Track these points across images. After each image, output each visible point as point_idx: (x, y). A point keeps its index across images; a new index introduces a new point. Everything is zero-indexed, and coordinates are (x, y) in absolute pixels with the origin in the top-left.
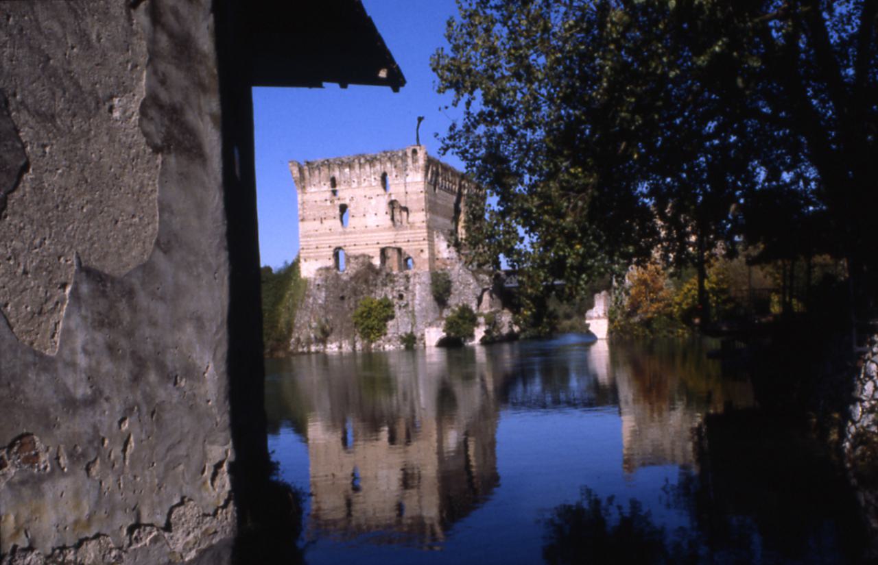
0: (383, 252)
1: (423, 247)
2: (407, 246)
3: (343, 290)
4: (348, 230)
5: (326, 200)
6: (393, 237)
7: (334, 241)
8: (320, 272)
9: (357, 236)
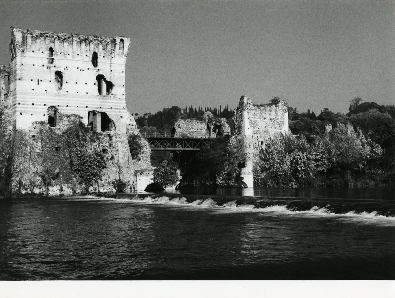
2: (110, 112)
3: (58, 142)
5: (43, 66)
6: (100, 103)
8: (35, 125)
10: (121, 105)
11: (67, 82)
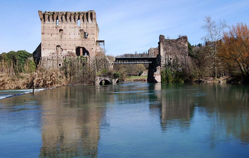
0: (78, 49)
4: (62, 39)
7: (56, 43)
9: (67, 41)
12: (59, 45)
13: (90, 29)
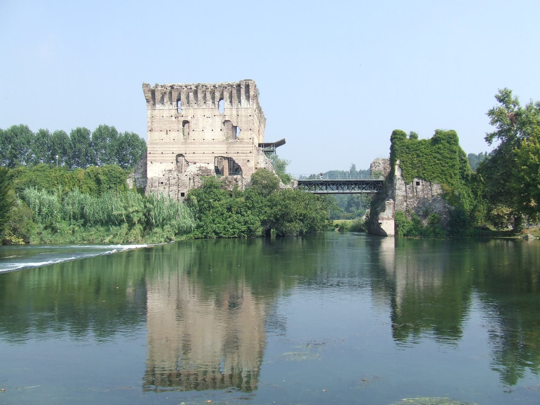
1: (249, 158)
4: (189, 141)
7: (176, 149)
10: (248, 149)
11: (193, 130)
12: (180, 153)
13: (244, 119)
